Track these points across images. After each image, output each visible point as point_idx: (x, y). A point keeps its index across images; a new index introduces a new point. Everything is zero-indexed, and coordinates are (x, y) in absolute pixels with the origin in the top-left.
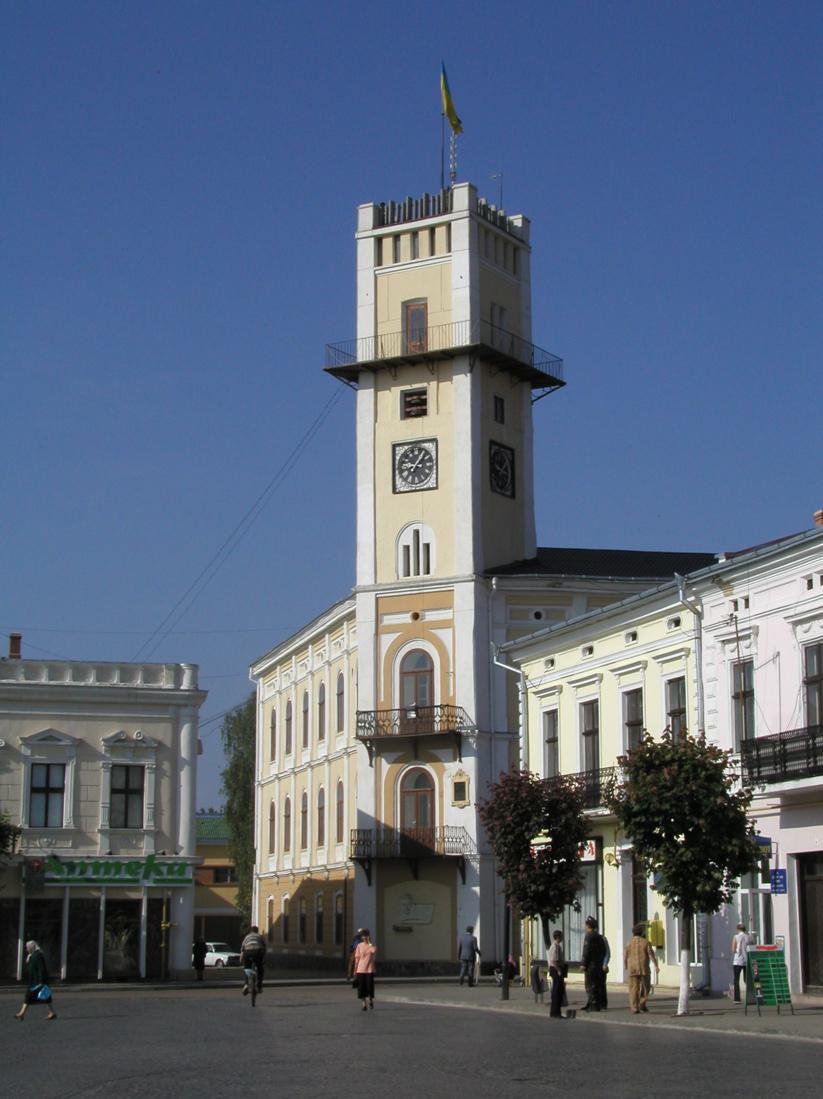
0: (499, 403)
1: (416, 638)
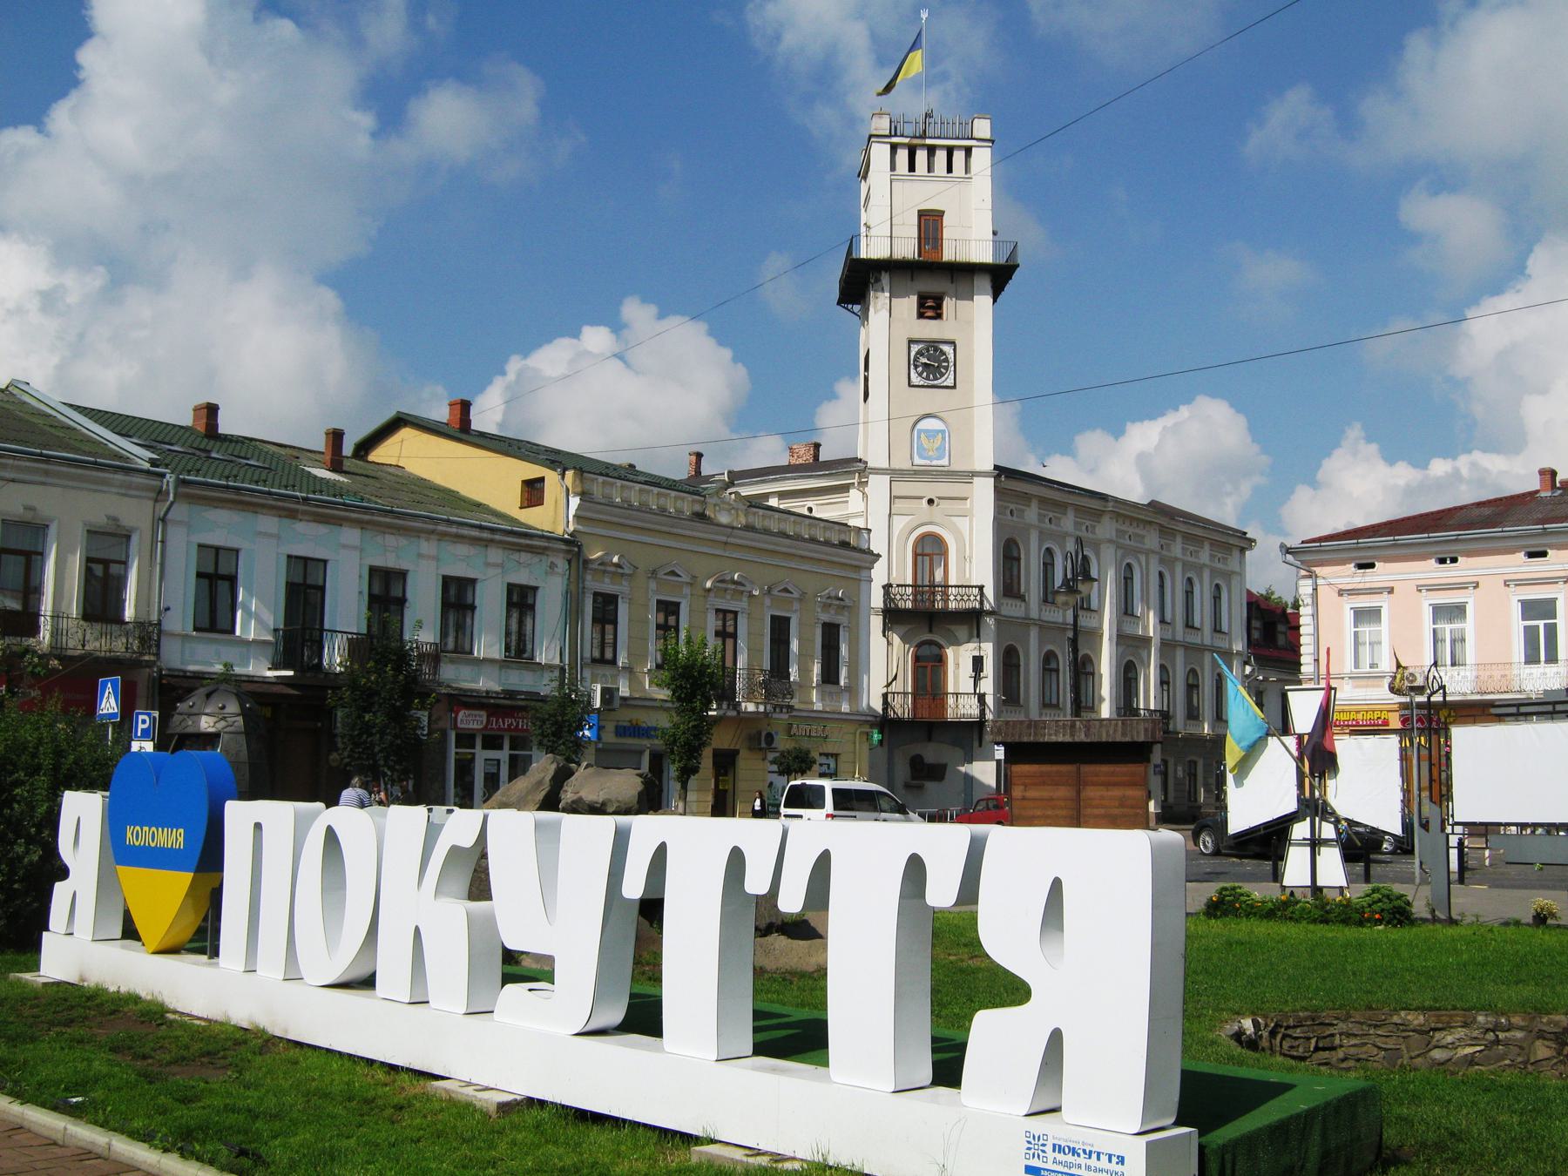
1: (931, 523)
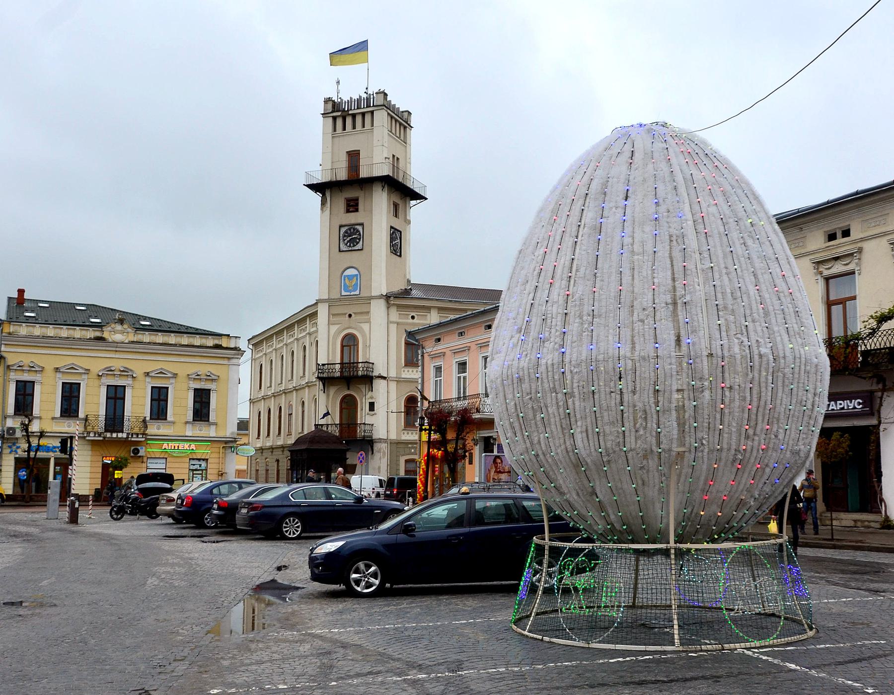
0: (396, 206)
